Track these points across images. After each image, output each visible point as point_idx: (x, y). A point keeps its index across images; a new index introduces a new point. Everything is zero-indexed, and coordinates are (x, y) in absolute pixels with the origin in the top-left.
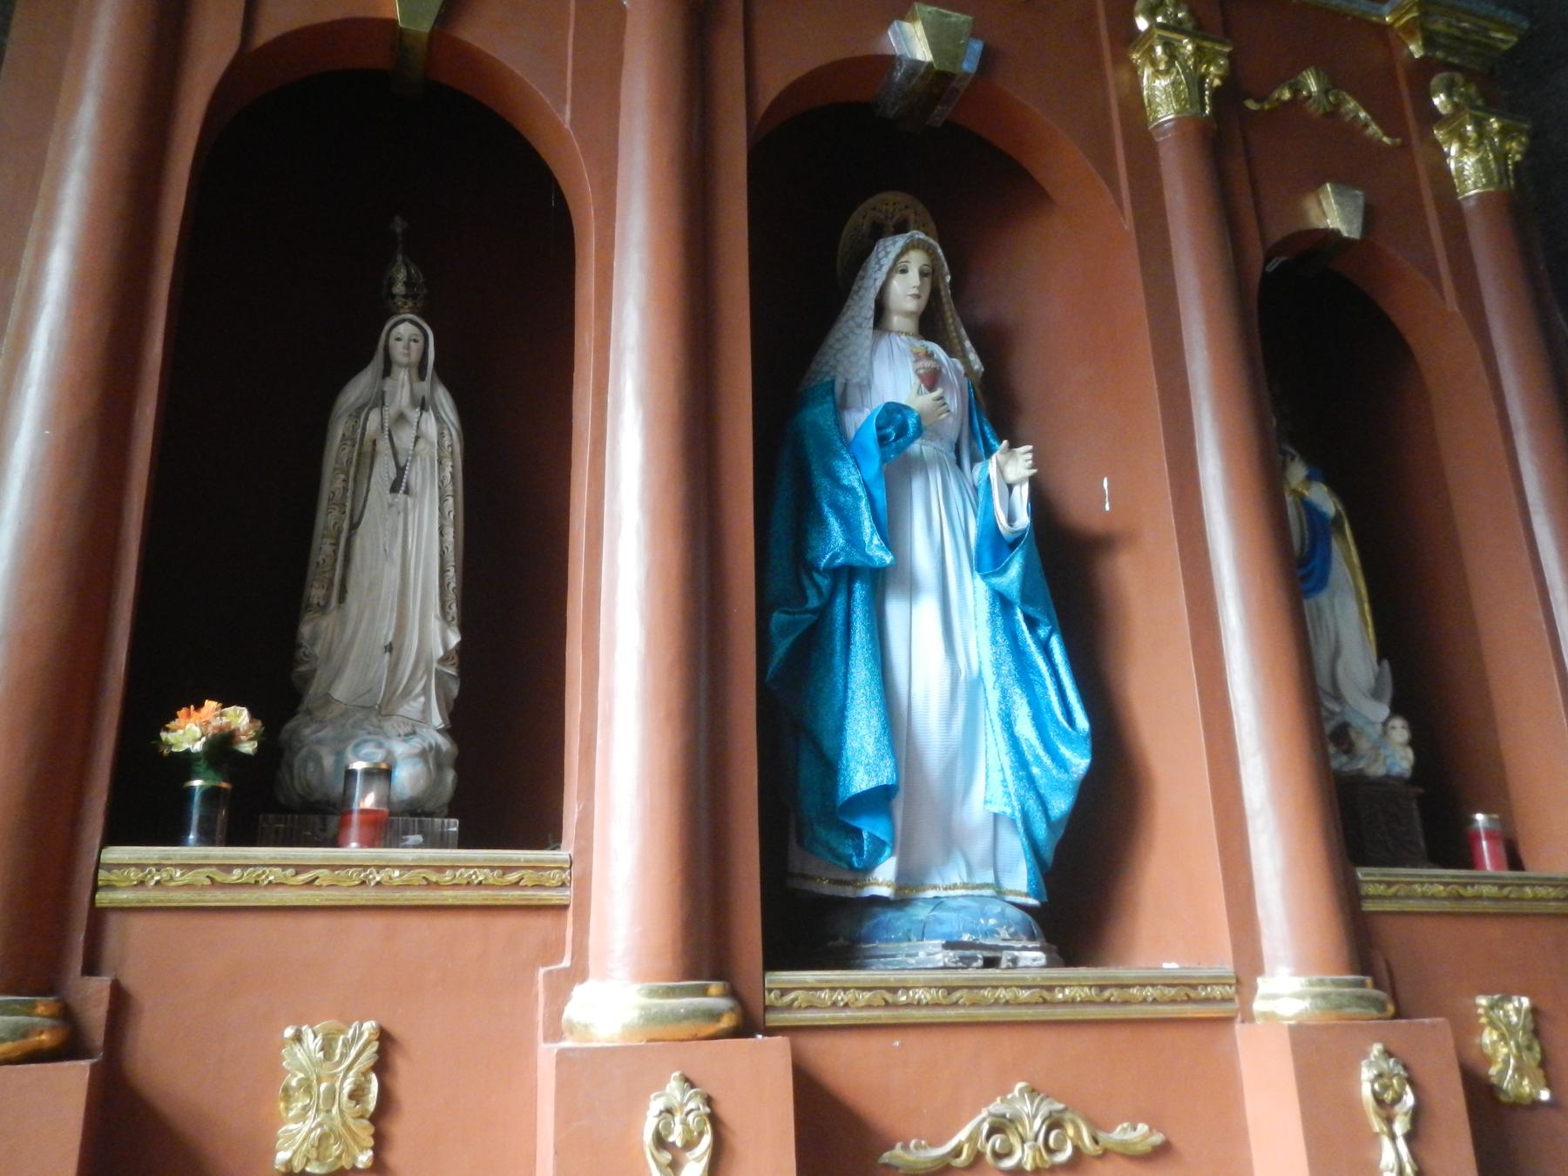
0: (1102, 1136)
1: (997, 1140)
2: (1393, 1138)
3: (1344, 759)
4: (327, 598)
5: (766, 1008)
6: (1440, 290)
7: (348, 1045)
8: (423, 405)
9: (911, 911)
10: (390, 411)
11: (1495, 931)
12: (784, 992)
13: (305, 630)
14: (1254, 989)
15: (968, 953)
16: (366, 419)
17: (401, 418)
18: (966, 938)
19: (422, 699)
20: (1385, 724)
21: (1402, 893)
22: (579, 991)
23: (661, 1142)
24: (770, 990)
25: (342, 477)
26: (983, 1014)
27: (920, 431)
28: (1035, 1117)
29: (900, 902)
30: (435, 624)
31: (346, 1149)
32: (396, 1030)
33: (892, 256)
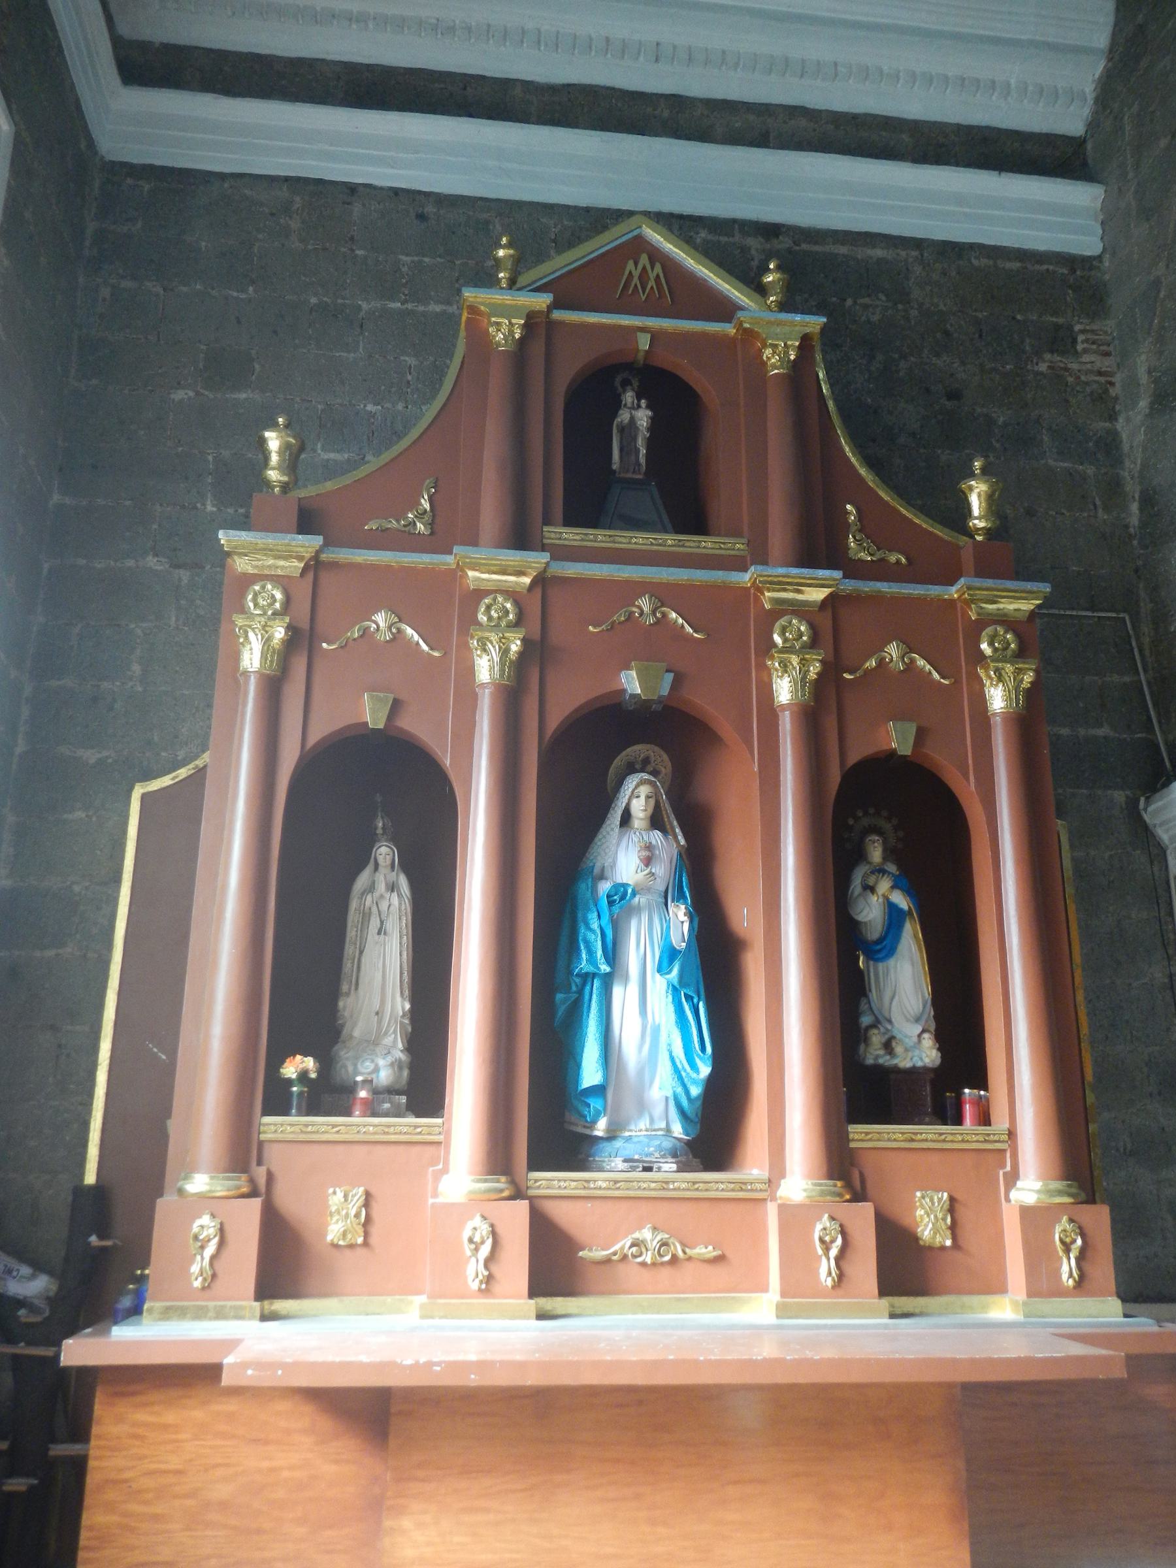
0: (687, 1250)
1: (634, 1249)
2: (828, 1259)
3: (888, 1057)
4: (350, 989)
5: (528, 1188)
6: (968, 780)
7: (353, 1196)
8: (392, 887)
9: (614, 1142)
10: (376, 894)
11: (935, 1158)
12: (536, 1181)
13: (341, 1004)
14: (778, 1186)
15: (635, 1164)
16: (365, 899)
17: (382, 896)
18: (636, 1157)
19: (393, 1036)
20: (919, 1036)
21: (875, 1138)
22: (445, 1177)
23: (471, 1241)
24: (530, 1180)
25: (355, 929)
26: (631, 1193)
27: (634, 894)
28: (653, 1240)
29: (611, 1137)
30: (399, 999)
31: (353, 1236)
32: (373, 1191)
33: (630, 790)
